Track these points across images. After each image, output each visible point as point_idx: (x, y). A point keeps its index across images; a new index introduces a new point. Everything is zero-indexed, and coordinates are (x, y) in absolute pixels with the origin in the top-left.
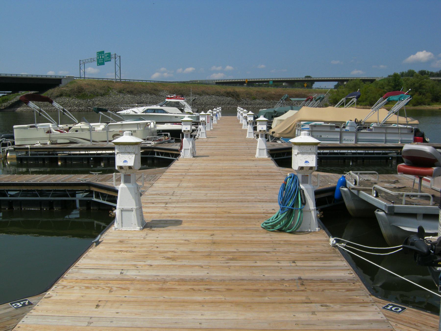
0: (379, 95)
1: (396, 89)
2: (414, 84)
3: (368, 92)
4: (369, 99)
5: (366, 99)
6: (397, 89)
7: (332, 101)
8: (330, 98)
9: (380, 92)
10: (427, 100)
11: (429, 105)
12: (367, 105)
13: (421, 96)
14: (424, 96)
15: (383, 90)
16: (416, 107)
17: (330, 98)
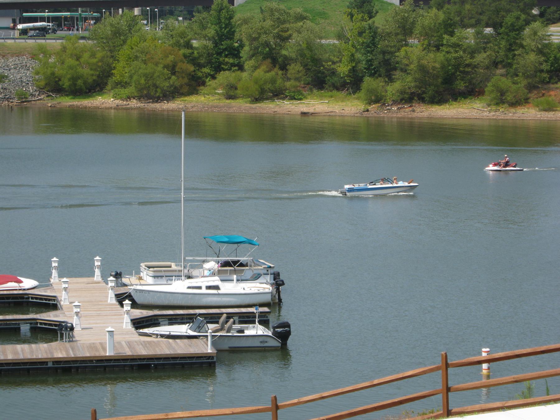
0: (165, 67)
1: (222, 47)
2: (259, 34)
3: (136, 57)
4: (135, 77)
5: (131, 77)
6: (224, 47)
7: (42, 83)
8: (37, 73)
9: (171, 58)
10: (288, 84)
11: (293, 98)
12: (134, 98)
13: (273, 73)
14: (280, 72)
15: (183, 51)
16: (254, 106)
17: (37, 73)
